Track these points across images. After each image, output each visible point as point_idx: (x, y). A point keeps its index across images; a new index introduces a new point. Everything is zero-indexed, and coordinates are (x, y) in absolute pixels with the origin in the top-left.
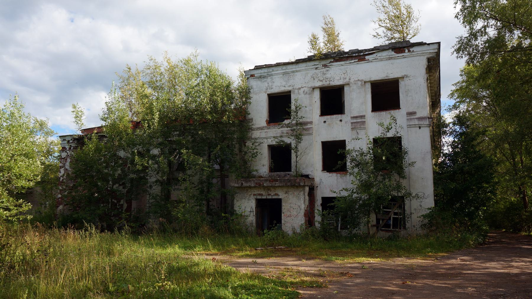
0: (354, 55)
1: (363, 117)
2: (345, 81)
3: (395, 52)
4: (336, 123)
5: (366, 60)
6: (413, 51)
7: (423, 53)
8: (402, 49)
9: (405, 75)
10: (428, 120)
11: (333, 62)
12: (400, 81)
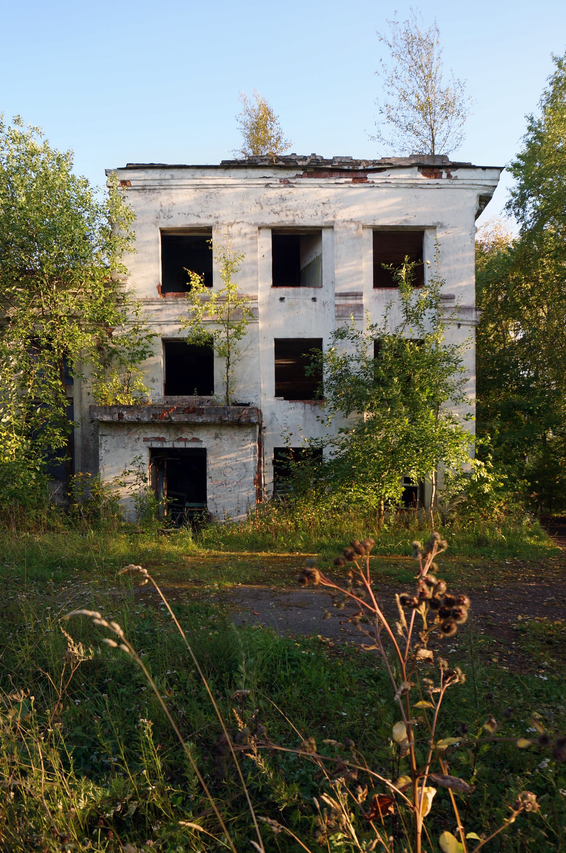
0: (346, 167)
1: (358, 295)
2: (326, 220)
3: (424, 174)
4: (305, 304)
5: (368, 182)
6: (456, 177)
7: (473, 184)
8: (436, 171)
9: (438, 223)
10: (474, 313)
11: (301, 176)
12: (427, 233)
